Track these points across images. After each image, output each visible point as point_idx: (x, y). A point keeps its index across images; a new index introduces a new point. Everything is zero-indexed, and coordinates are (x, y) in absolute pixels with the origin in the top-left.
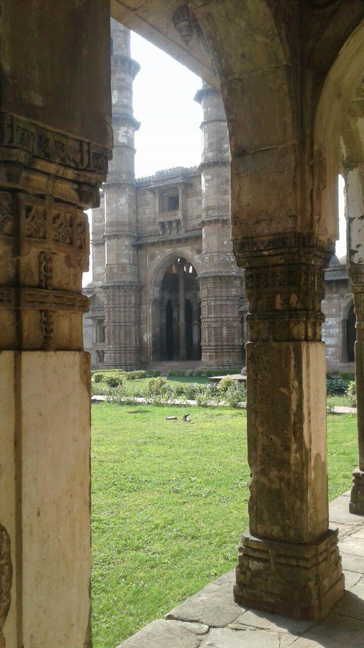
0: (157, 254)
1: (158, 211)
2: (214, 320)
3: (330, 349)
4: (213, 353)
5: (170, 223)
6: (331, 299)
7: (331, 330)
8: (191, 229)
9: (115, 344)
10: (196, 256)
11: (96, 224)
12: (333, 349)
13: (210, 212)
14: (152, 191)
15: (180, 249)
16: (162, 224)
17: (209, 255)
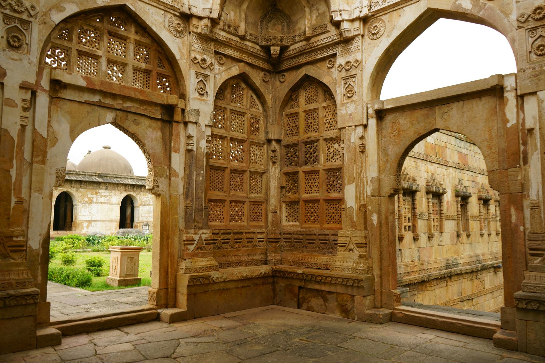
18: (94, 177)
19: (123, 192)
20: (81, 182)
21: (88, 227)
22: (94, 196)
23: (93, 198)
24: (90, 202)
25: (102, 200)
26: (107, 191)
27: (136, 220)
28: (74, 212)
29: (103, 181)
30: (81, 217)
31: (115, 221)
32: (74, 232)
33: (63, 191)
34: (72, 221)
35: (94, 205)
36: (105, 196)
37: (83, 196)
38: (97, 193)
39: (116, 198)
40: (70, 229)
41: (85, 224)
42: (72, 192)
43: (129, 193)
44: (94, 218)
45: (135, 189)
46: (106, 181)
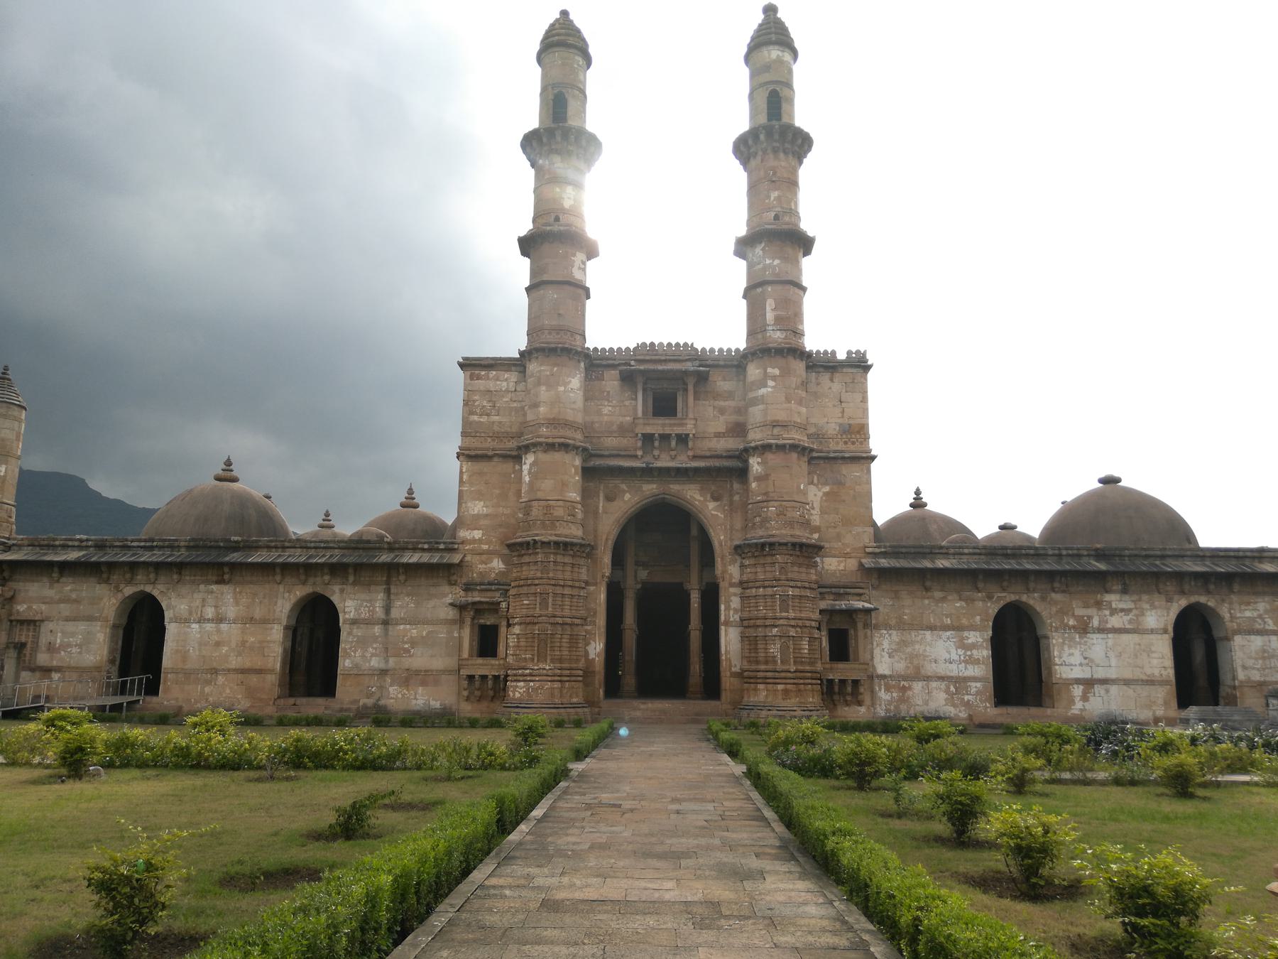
0: (624, 492)
1: (640, 413)
2: (793, 623)
3: (973, 684)
4: (789, 687)
5: (665, 438)
6: (974, 600)
7: (975, 652)
8: (708, 454)
9: (552, 661)
10: (712, 505)
11: (476, 418)
12: (978, 685)
13: (776, 431)
14: (628, 378)
15: (675, 488)
16: (648, 438)
17: (776, 504)
18: (1085, 560)
19: (1176, 597)
20: (1051, 576)
21: (1085, 698)
22: (1092, 611)
23: (1090, 618)
24: (1084, 628)
25: (1115, 621)
26: (1126, 597)
27: (1225, 678)
28: (1044, 656)
29: (1111, 568)
30: (1064, 669)
31: (1163, 683)
32: (1049, 711)
33: (1008, 600)
34: (1041, 681)
35: (1095, 638)
36: (1122, 610)
37: (1063, 612)
38: (1099, 605)
39: (1159, 616)
40: (1039, 703)
41: (1077, 691)
42: (1031, 602)
43: (1194, 599)
44: (1100, 674)
45: (1212, 587)
46: (1122, 569)
